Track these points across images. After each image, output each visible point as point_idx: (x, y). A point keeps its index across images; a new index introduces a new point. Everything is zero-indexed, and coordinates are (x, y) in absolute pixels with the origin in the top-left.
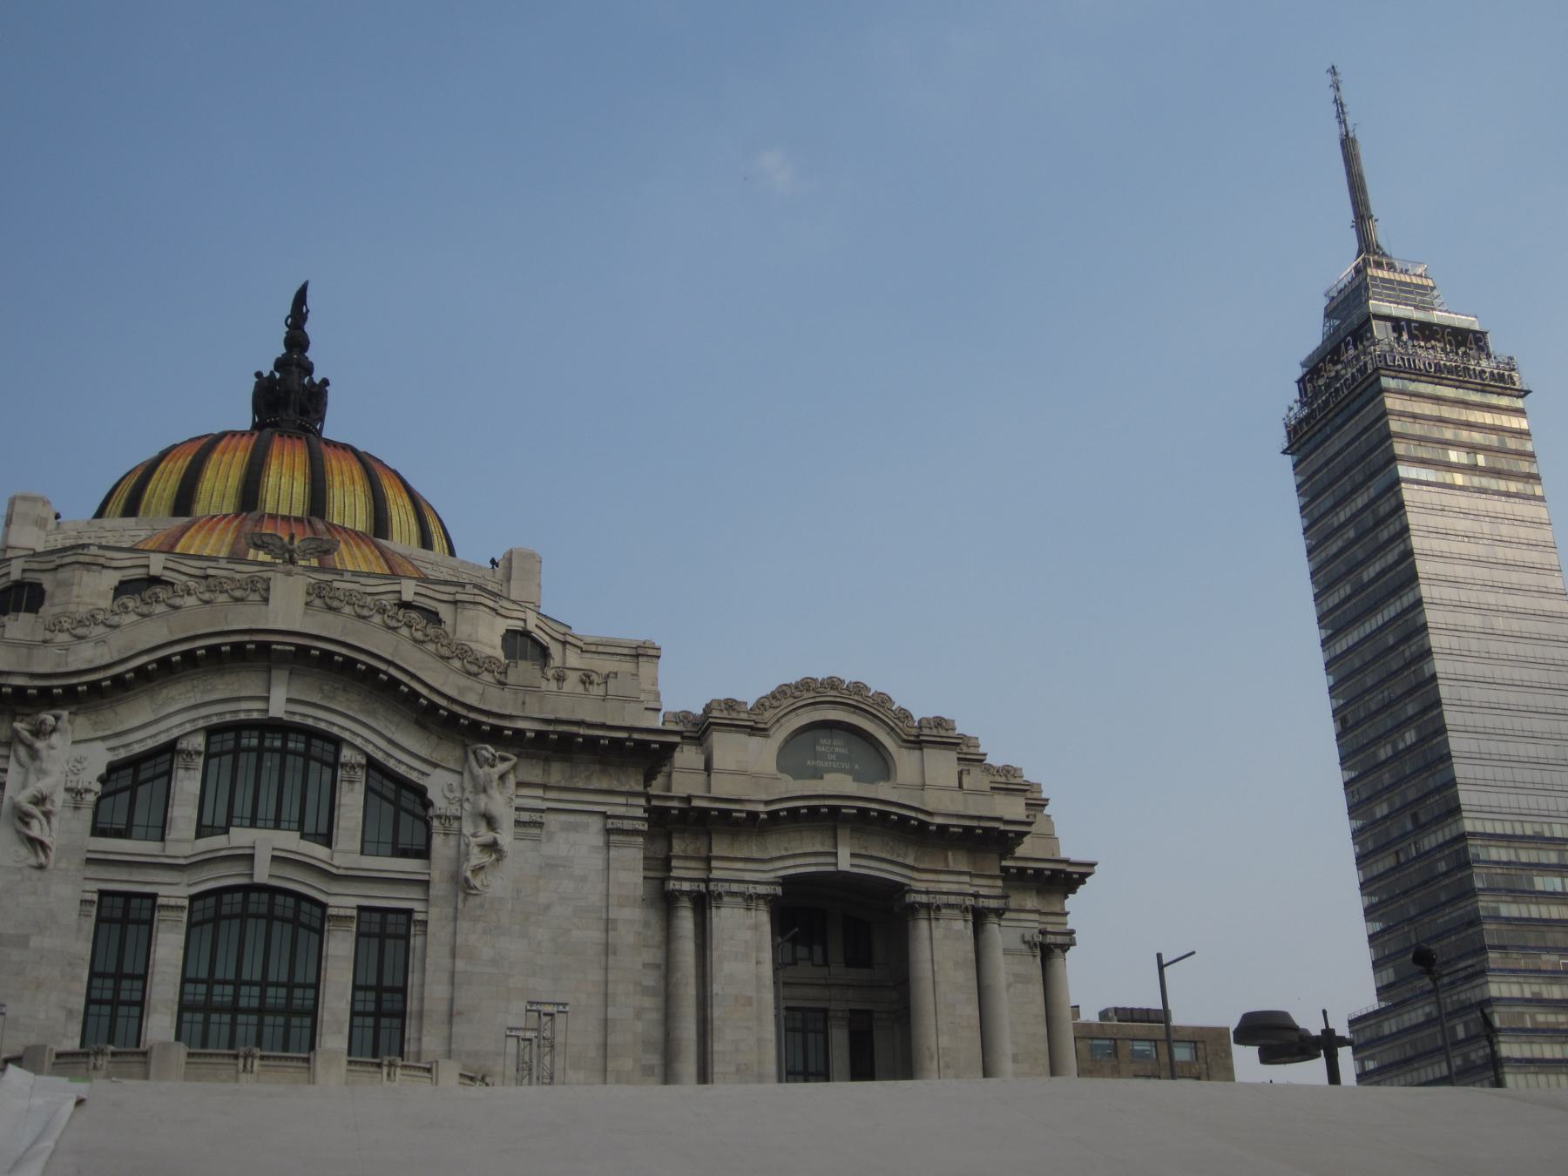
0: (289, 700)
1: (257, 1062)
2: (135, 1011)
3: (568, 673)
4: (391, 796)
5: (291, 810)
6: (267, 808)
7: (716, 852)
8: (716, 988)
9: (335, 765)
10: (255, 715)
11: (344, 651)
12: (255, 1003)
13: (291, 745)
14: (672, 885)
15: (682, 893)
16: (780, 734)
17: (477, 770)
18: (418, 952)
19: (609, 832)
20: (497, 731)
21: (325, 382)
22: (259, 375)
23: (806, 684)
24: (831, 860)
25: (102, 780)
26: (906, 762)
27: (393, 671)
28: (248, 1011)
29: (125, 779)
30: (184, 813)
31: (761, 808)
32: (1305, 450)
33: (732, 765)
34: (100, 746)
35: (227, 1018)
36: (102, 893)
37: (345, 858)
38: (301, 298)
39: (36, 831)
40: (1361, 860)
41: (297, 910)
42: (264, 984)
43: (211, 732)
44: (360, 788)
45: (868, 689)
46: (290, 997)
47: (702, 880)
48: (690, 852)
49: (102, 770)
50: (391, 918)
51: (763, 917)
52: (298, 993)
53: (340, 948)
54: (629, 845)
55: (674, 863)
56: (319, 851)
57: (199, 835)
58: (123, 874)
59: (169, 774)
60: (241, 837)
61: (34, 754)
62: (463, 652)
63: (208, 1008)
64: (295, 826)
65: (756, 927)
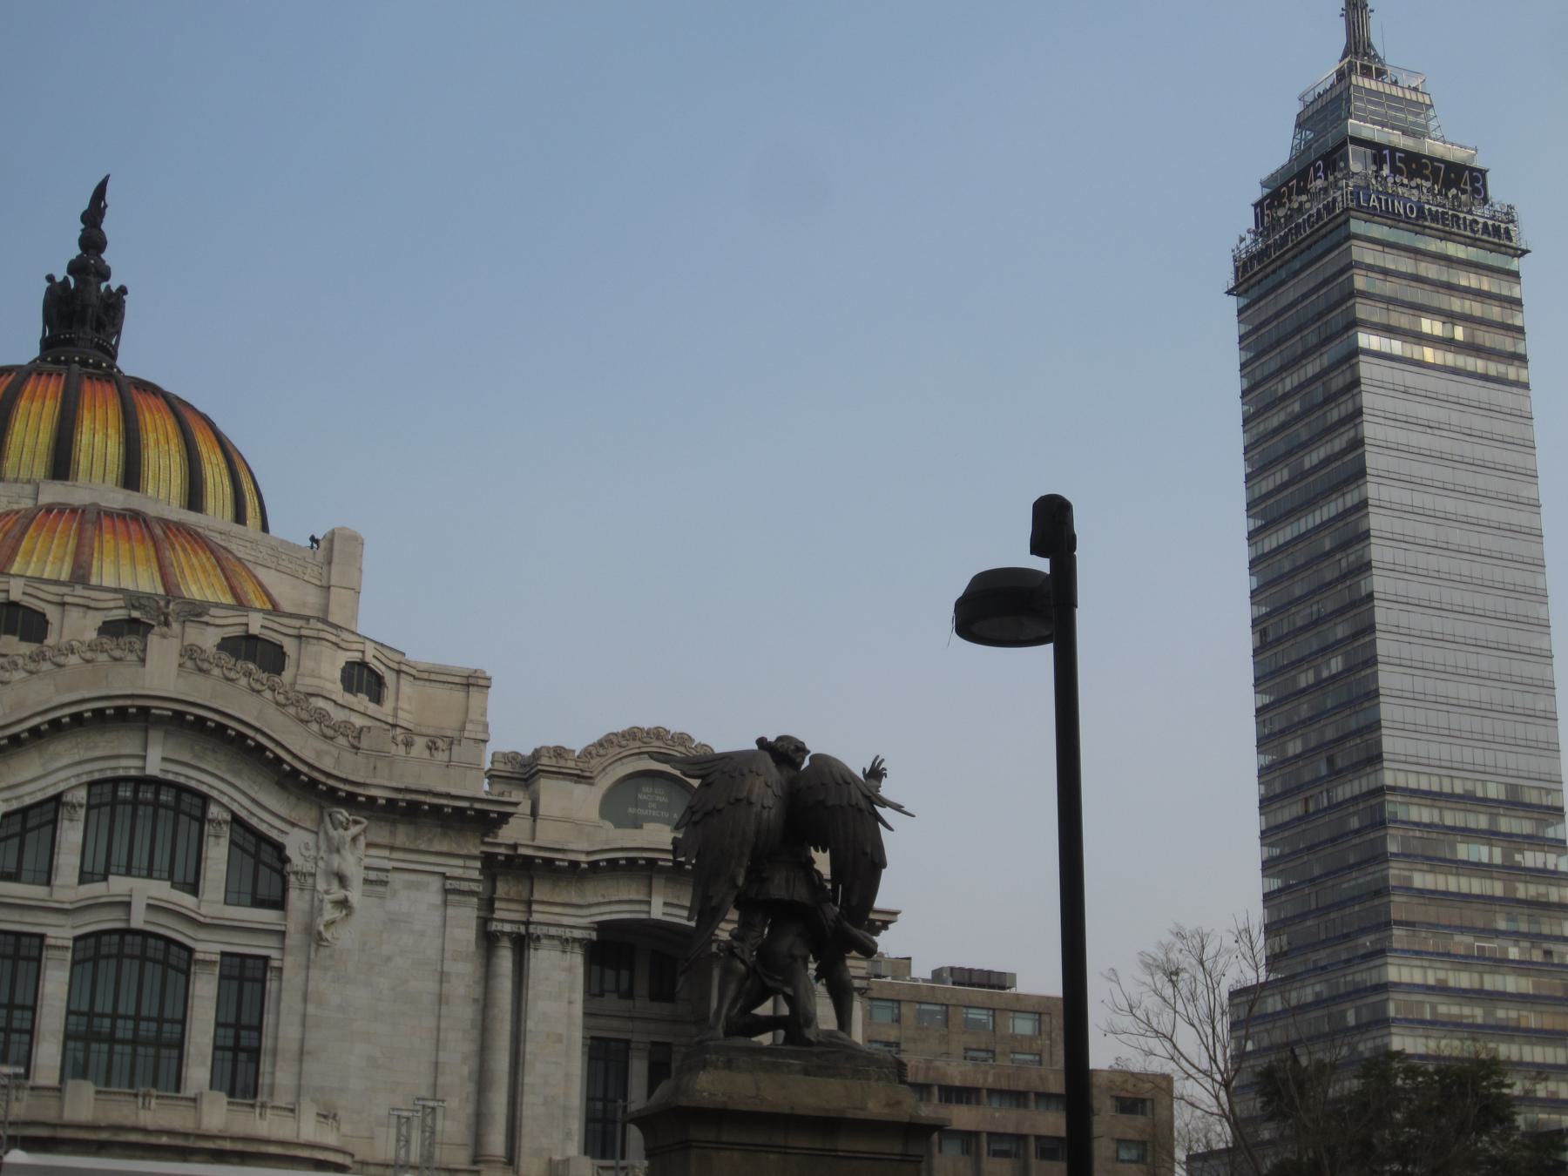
0: (164, 759)
1: (153, 1101)
3: (416, 738)
4: (252, 849)
5: (161, 859)
7: (537, 896)
8: (530, 1025)
9: (202, 819)
10: (133, 772)
11: (217, 718)
12: (129, 1035)
13: (163, 798)
14: (495, 926)
15: (503, 933)
16: (604, 784)
18: (274, 995)
19: (446, 891)
20: (352, 797)
21: (123, 290)
22: (50, 278)
23: (632, 734)
24: (645, 908)
28: (123, 1042)
31: (582, 858)
32: (1254, 293)
35: (105, 1047)
37: (209, 910)
38: (100, 192)
40: (1266, 803)
41: (167, 953)
42: (137, 1018)
43: (91, 785)
45: (692, 740)
46: (160, 1030)
48: (513, 895)
50: (249, 962)
51: (577, 959)
52: (167, 1027)
53: (205, 990)
55: (497, 905)
56: (187, 900)
57: (82, 881)
58: (15, 915)
59: (54, 823)
60: (119, 885)
64: (166, 875)
65: (570, 969)
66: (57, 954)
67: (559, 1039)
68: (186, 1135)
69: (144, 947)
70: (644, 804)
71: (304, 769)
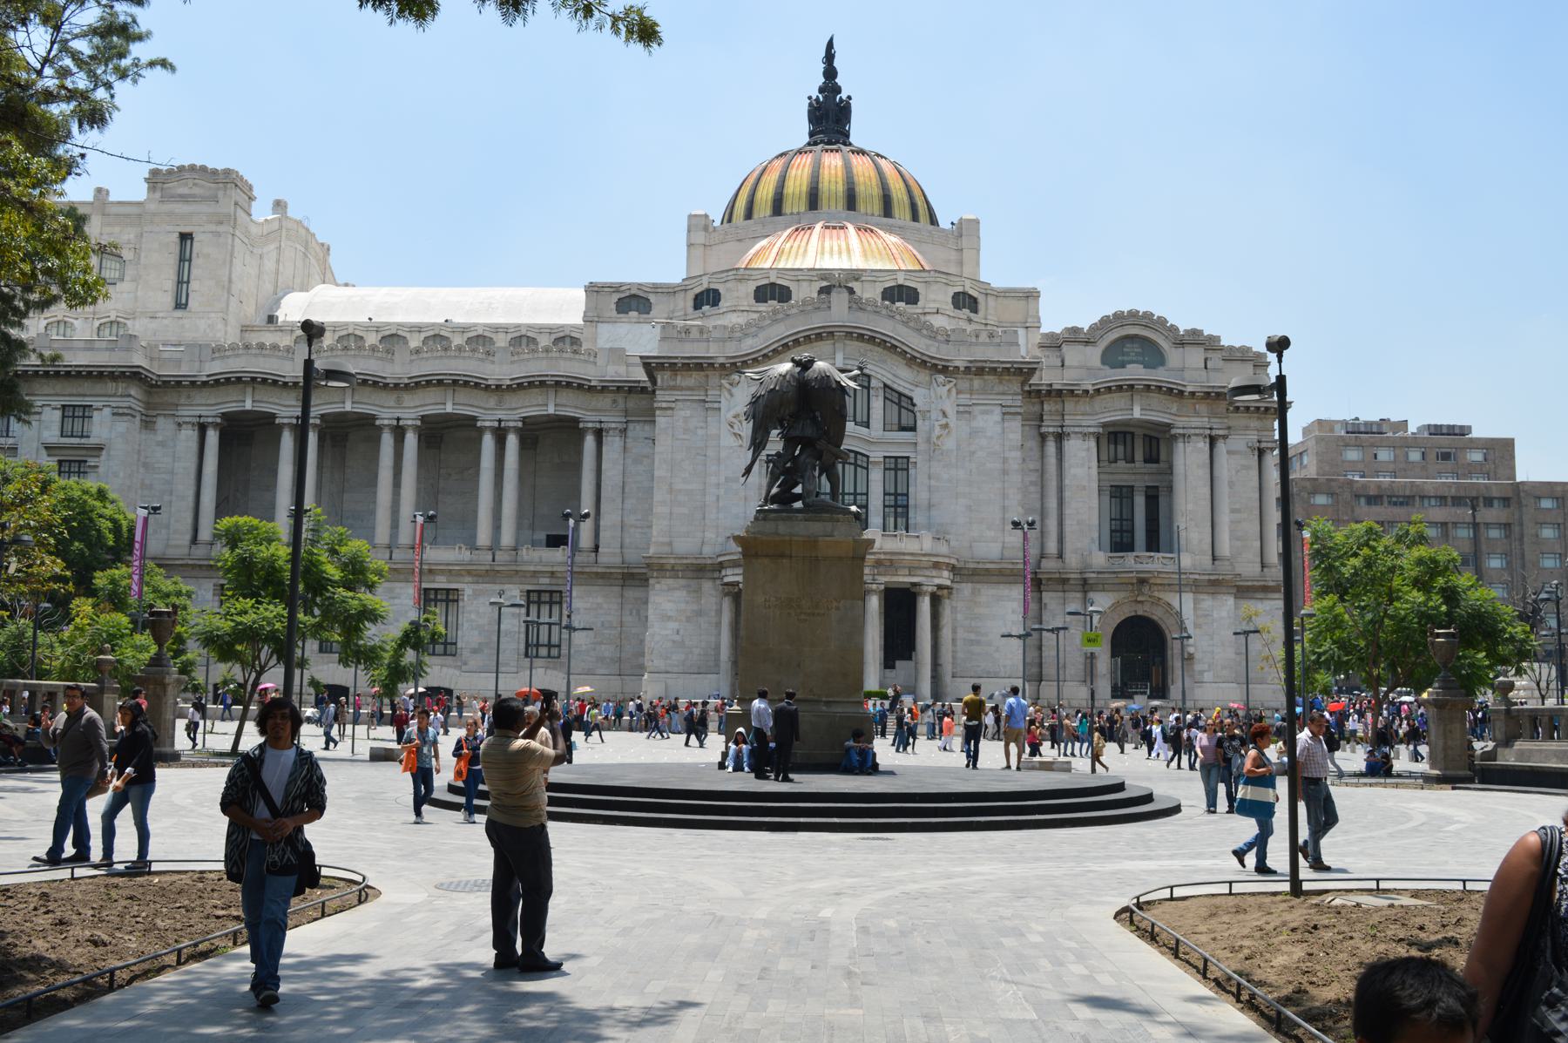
8: (1067, 482)
14: (1043, 430)
16: (1103, 344)
26: (1174, 356)
31: (1090, 388)
38: (830, 45)
44: (881, 399)
53: (876, 475)
67: (1084, 488)
70: (1128, 354)
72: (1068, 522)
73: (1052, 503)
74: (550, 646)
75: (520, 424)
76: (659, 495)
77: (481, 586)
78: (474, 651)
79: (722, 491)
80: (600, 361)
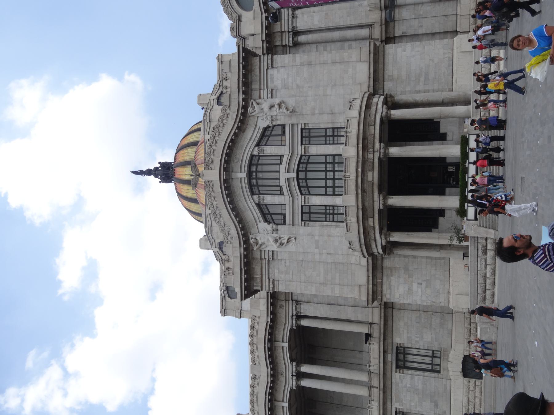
1: (347, 174)
2: (335, 208)
4: (267, 138)
5: (274, 168)
6: (274, 175)
7: (279, 30)
8: (323, 26)
10: (246, 181)
11: (224, 157)
12: (332, 173)
13: (254, 170)
14: (291, 44)
17: (257, 112)
18: (314, 125)
21: (160, 163)
22: (160, 182)
25: (269, 223)
27: (228, 141)
28: (334, 175)
29: (269, 217)
30: (277, 200)
31: (264, 16)
33: (252, 27)
34: (259, 225)
36: (302, 220)
38: (136, 173)
39: (285, 241)
43: (253, 194)
44: (265, 148)
46: (330, 163)
47: (289, 34)
48: (280, 39)
49: (266, 224)
52: (328, 161)
53: (313, 150)
54: (276, 60)
55: (284, 44)
56: (285, 159)
57: (283, 194)
58: (296, 215)
59: (266, 205)
61: (263, 244)
62: (221, 119)
63: (334, 187)
66: (307, 200)
67: (327, 14)
68: (357, 162)
69: (302, 171)
71: (236, 125)
72: (349, 23)
73: (336, 35)
74: (433, 357)
75: (294, 364)
76: (327, 292)
77: (394, 397)
78: (436, 405)
79: (324, 251)
80: (258, 314)
